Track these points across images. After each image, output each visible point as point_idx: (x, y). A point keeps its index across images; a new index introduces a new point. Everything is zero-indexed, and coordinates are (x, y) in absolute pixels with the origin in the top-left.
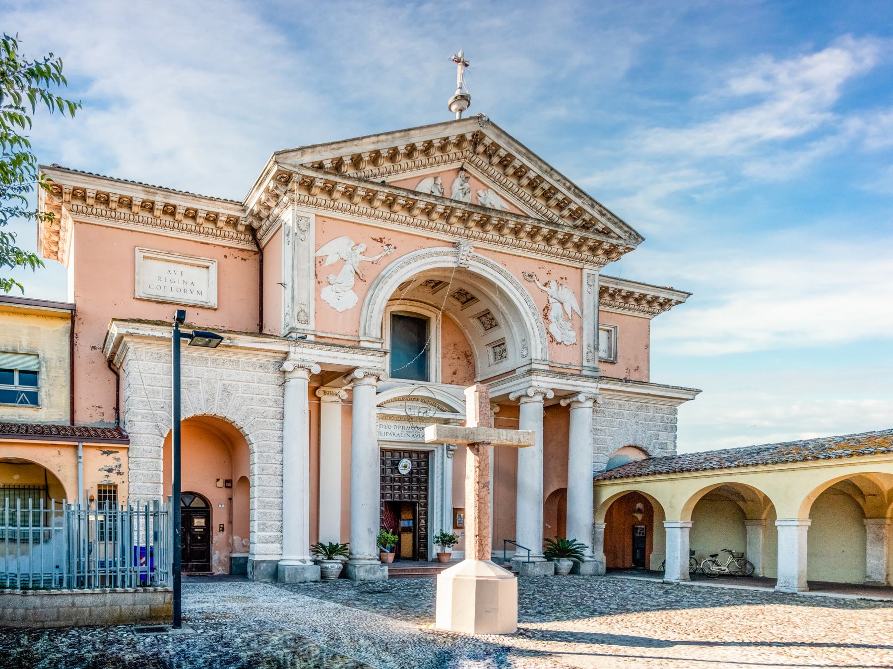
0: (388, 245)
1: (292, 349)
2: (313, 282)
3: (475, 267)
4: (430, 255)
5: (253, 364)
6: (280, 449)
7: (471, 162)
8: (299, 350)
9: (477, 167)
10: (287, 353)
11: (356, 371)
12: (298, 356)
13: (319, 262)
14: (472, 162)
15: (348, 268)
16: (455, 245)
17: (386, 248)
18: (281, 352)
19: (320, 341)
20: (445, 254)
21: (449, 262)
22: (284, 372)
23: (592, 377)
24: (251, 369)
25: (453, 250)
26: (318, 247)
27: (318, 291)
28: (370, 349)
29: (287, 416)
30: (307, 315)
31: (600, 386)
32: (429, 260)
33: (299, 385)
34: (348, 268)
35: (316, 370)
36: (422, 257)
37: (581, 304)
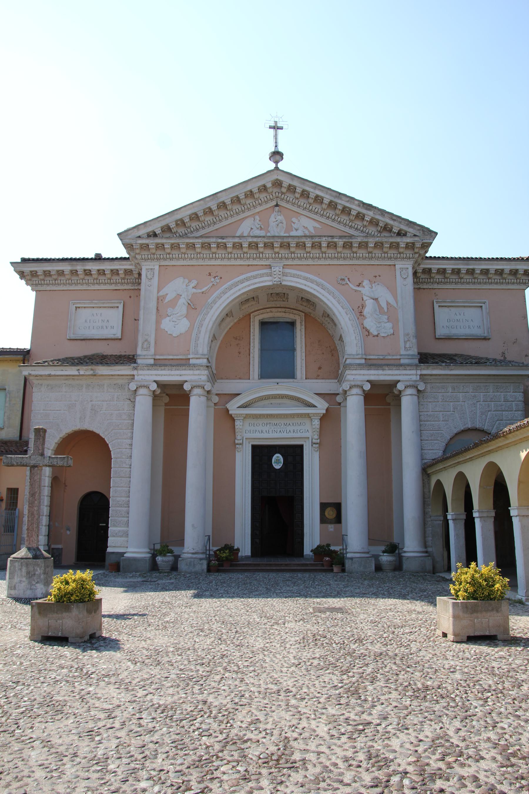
1: (135, 372)
4: (247, 279)
7: (282, 199)
8: (141, 372)
9: (288, 202)
12: (141, 377)
14: (283, 199)
15: (182, 301)
16: (270, 267)
17: (213, 279)
18: (130, 375)
20: (262, 276)
21: (267, 281)
23: (408, 365)
25: (268, 271)
27: (158, 322)
30: (149, 343)
31: (419, 372)
34: (182, 301)
36: (242, 282)
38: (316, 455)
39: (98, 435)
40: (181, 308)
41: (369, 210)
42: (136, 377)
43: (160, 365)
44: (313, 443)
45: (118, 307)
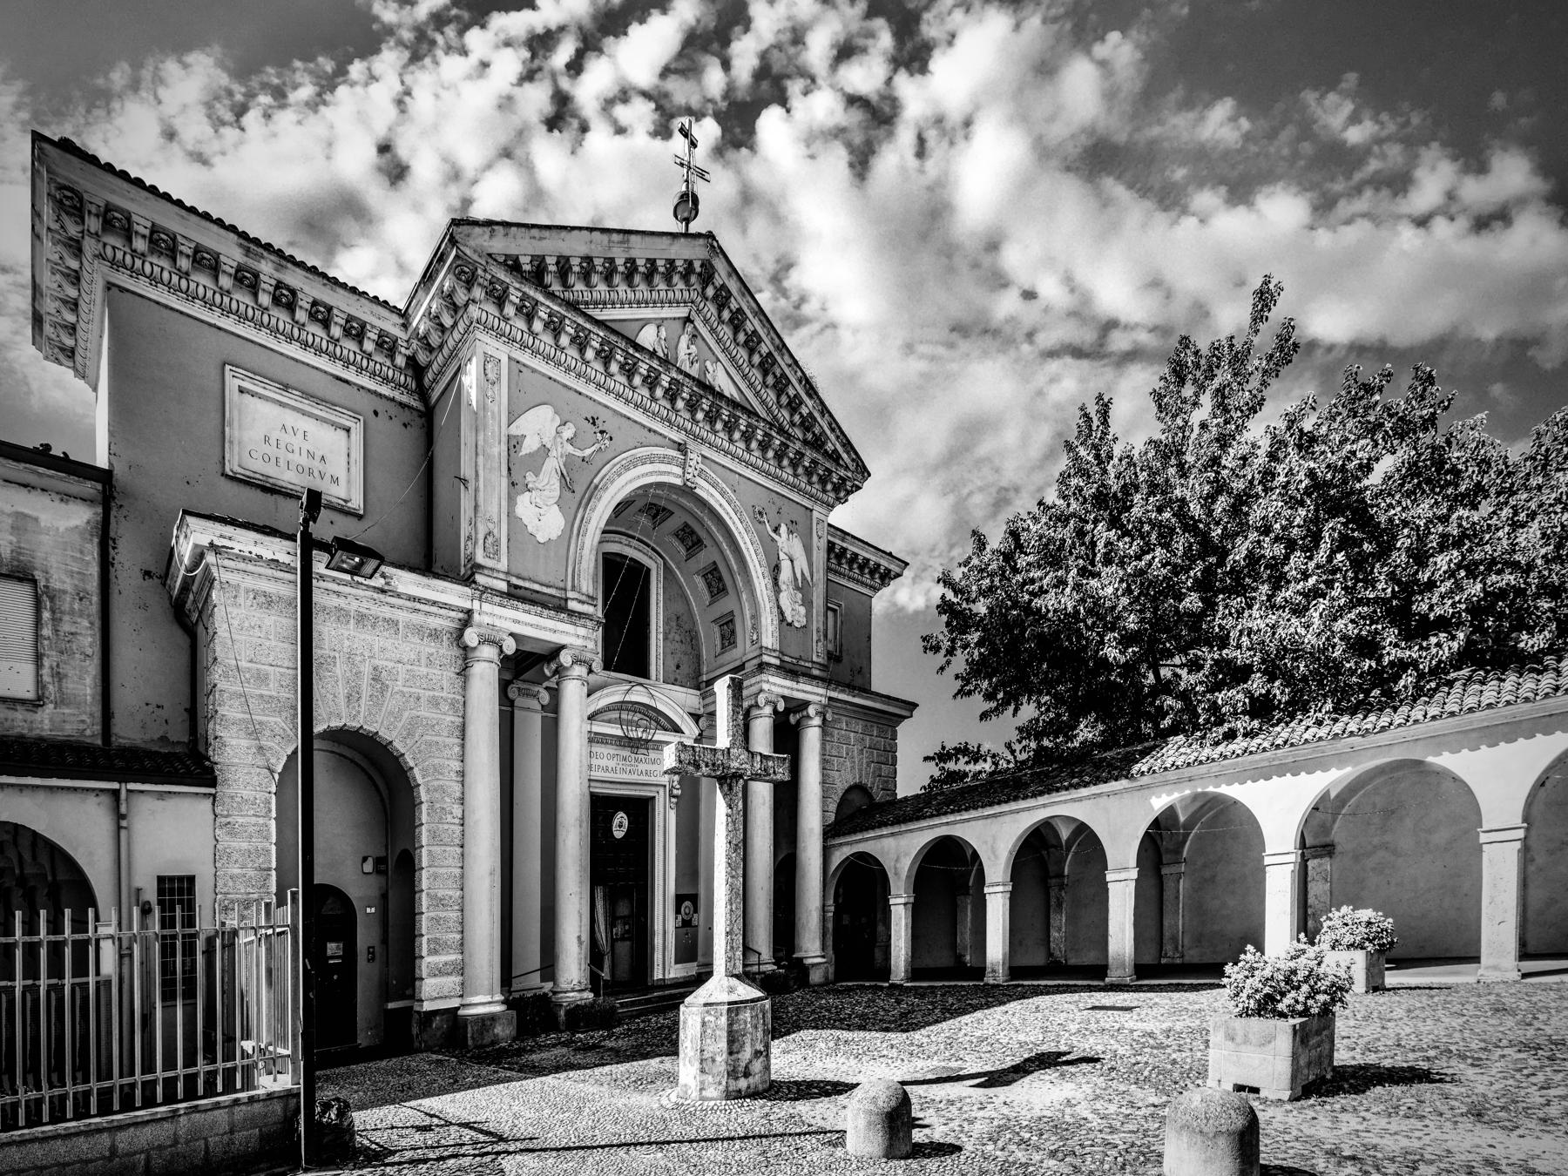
0: (602, 432)
2: (505, 482)
3: (705, 491)
5: (419, 630)
6: (458, 794)
8: (486, 607)
10: (469, 612)
11: (563, 652)
12: (487, 619)
13: (514, 443)
15: (552, 464)
19: (515, 594)
22: (465, 648)
24: (416, 640)
26: (512, 418)
27: (511, 501)
28: (581, 615)
29: (471, 731)
30: (497, 543)
32: (648, 468)
33: (485, 675)
34: (552, 464)
35: (510, 647)
37: (810, 565)
38: (672, 816)
39: (1470, 792)
40: (548, 481)
41: (810, 397)
42: (476, 617)
43: (523, 600)
44: (672, 796)
45: (348, 430)
